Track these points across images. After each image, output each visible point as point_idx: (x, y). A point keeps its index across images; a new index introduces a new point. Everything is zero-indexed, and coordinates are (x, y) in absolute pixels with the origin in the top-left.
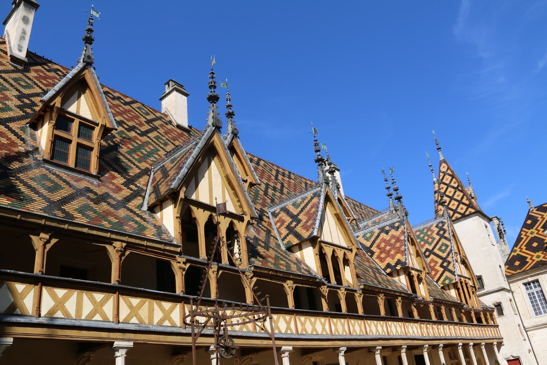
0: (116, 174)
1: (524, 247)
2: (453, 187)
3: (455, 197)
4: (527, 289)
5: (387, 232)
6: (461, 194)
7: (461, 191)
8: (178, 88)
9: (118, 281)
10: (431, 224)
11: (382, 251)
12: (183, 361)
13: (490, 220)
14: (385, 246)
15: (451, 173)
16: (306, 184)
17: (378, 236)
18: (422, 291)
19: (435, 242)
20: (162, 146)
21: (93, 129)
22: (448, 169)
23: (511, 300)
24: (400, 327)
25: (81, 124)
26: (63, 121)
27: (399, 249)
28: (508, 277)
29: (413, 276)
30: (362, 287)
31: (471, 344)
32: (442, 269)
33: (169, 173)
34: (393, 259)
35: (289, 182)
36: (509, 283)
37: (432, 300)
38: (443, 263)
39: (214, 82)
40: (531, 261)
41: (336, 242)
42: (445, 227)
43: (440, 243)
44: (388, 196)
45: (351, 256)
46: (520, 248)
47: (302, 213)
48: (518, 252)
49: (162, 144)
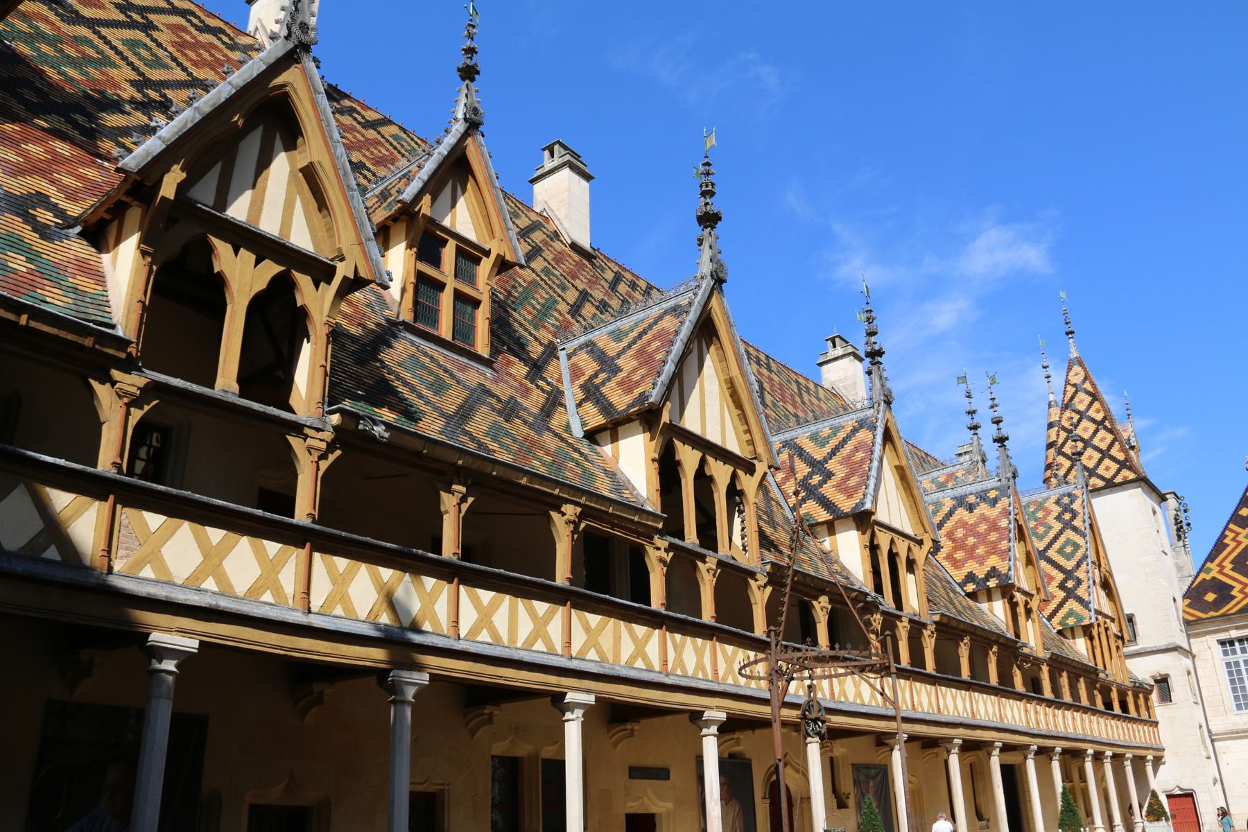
0: (512, 358)
1: (1228, 565)
2: (1093, 420)
3: (1096, 442)
4: (1225, 653)
5: (971, 508)
6: (1110, 437)
7: (1111, 431)
8: (574, 161)
9: (569, 580)
10: (1045, 495)
11: (959, 545)
12: (632, 735)
13: (1162, 498)
14: (966, 536)
15: (1091, 389)
16: (798, 384)
17: (951, 513)
18: (1032, 638)
19: (1051, 535)
20: (559, 291)
21: (477, 261)
22: (1086, 378)
23: (1189, 673)
24: (993, 704)
25: (459, 252)
26: (428, 242)
27: (994, 545)
28: (1187, 623)
29: (1016, 604)
30: (937, 618)
31: (1109, 753)
32: (1062, 594)
33: (619, 362)
34: (982, 564)
35: (771, 379)
36: (1189, 637)
37: (1048, 656)
38: (1065, 580)
39: (713, 185)
40: (1240, 596)
41: (896, 524)
42: (1076, 506)
43: (1062, 539)
44: (970, 429)
45: (920, 554)
46: (1220, 565)
47: (834, 459)
48: (1214, 573)
49: (558, 286)
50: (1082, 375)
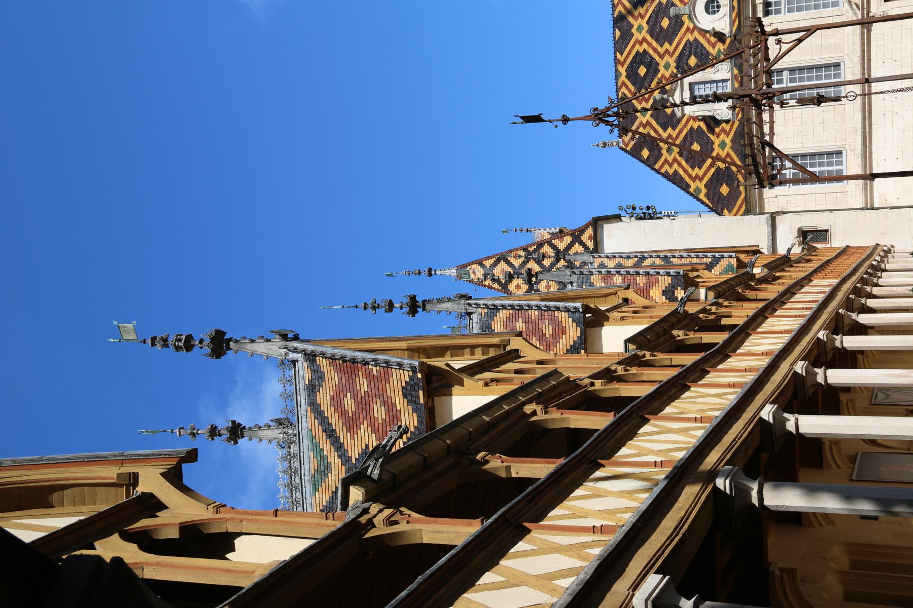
13: (618, 218)
28: (748, 212)
46: (694, 180)
48: (701, 185)
50: (476, 267)
